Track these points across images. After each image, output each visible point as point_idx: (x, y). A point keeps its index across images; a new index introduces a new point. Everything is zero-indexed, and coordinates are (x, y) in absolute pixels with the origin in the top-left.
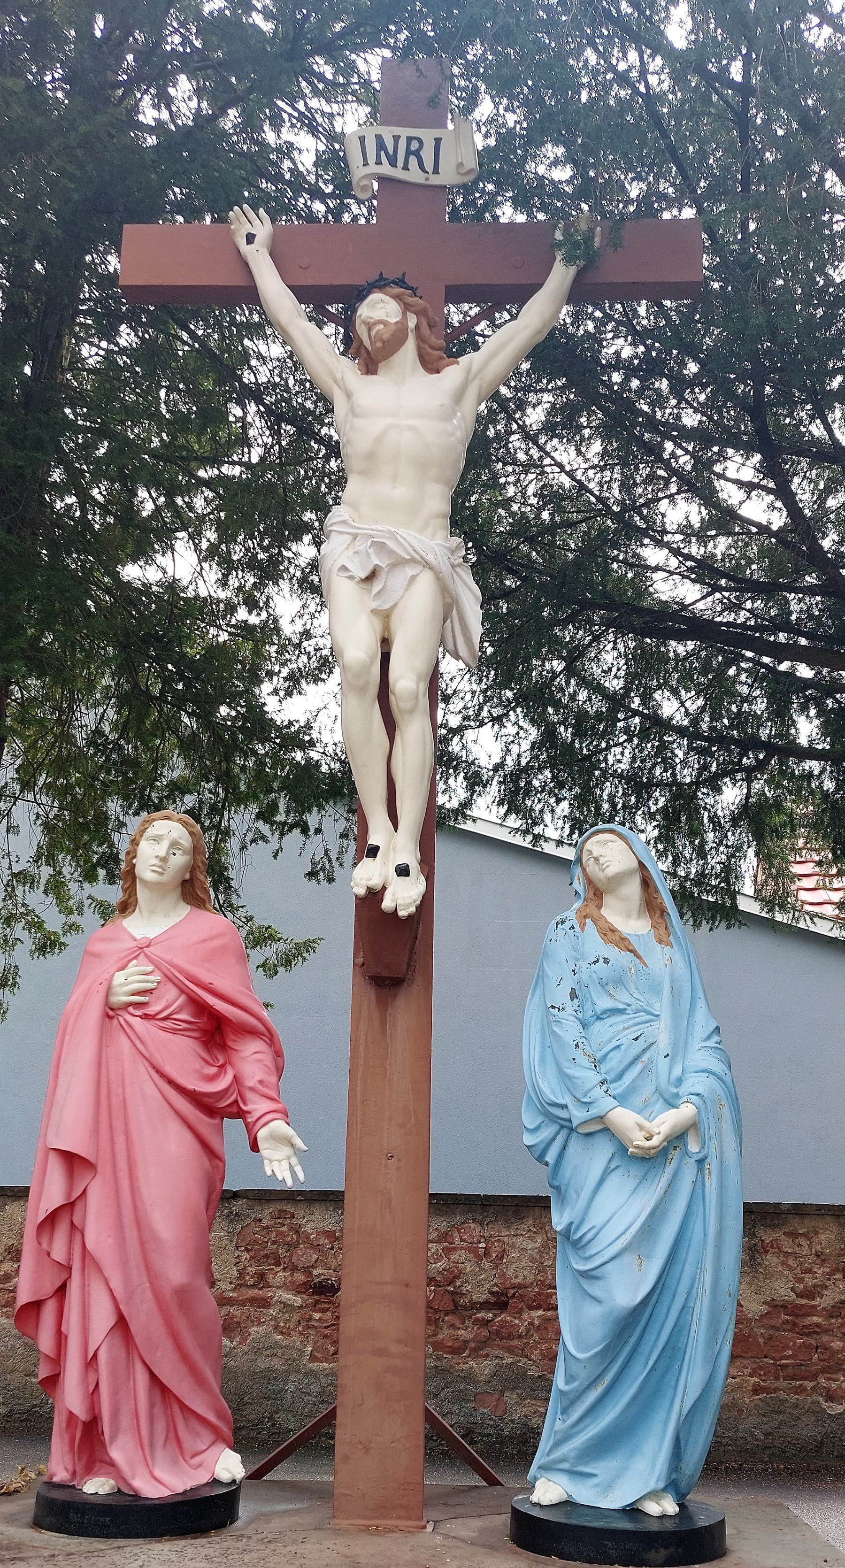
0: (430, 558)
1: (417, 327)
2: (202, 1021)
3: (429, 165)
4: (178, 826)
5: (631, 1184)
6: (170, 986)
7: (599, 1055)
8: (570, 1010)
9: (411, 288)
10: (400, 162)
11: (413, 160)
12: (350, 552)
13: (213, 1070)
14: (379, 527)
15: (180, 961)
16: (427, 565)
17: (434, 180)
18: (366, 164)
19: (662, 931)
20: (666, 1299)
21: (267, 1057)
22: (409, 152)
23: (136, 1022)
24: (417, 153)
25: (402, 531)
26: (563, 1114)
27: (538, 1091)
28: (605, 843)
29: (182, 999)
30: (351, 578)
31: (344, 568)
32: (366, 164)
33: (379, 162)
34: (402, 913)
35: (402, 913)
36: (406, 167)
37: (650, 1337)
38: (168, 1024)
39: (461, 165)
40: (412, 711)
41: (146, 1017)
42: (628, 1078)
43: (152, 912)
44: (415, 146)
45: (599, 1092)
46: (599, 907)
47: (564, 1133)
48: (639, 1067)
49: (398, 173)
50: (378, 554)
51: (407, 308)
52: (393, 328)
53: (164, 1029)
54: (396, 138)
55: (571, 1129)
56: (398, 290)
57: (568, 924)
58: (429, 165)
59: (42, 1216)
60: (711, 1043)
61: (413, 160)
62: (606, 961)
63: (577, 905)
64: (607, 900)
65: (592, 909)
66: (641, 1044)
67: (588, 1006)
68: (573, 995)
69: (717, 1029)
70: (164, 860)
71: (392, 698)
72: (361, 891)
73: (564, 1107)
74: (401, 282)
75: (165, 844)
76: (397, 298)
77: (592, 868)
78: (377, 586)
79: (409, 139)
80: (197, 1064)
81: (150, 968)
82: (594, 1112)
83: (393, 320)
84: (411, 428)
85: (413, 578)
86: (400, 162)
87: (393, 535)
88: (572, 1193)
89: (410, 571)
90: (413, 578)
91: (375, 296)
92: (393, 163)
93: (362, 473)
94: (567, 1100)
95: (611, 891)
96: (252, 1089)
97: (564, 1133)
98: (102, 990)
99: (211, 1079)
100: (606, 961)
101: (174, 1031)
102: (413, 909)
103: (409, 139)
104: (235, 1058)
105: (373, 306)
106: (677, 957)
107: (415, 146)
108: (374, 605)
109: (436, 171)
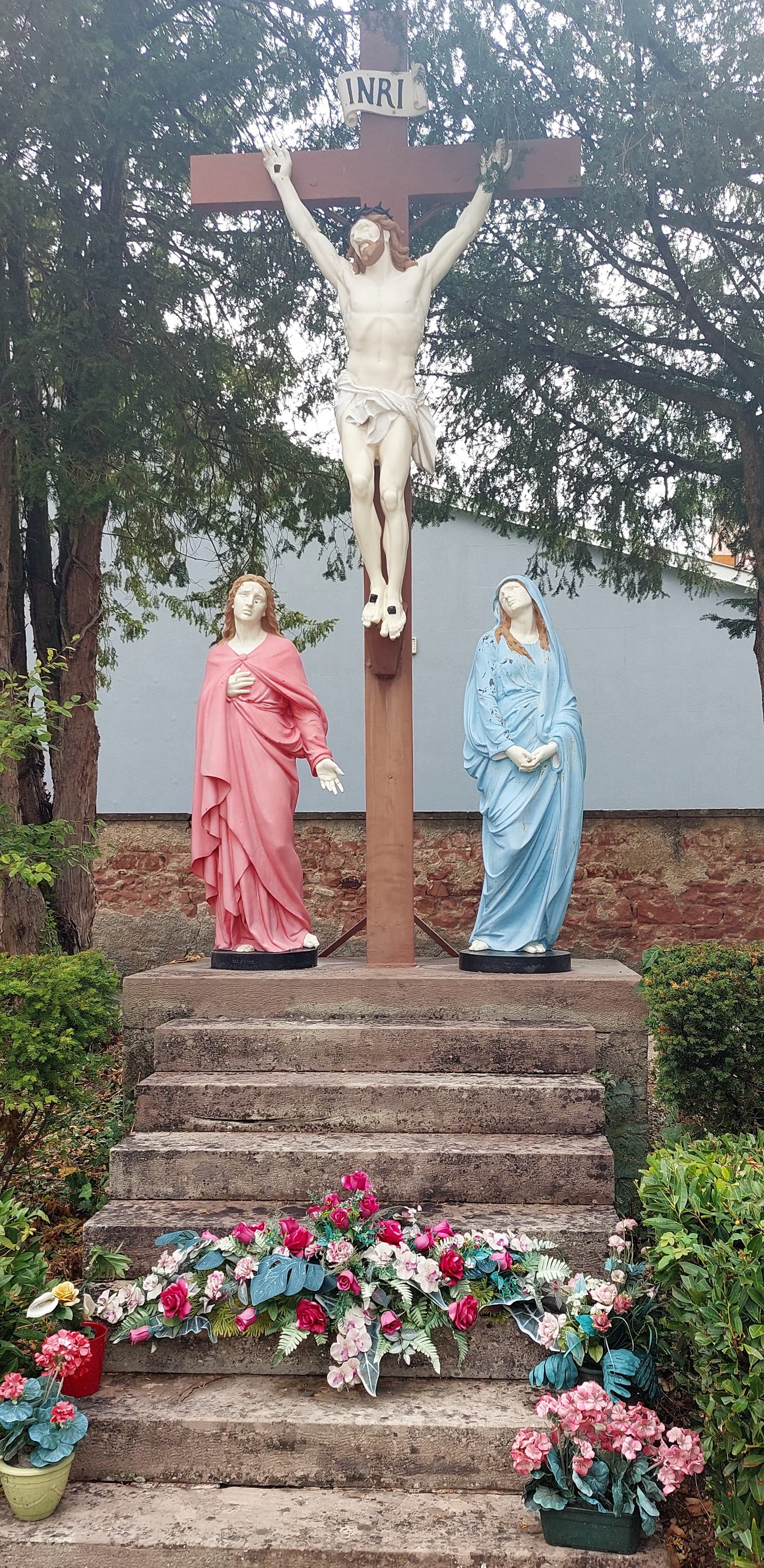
0: (403, 409)
1: (390, 239)
2: (280, 703)
3: (395, 102)
4: (258, 584)
5: (521, 786)
6: (261, 683)
7: (505, 717)
8: (489, 692)
9: (386, 213)
10: (375, 100)
11: (384, 97)
12: (353, 406)
13: (288, 731)
14: (370, 388)
15: (265, 668)
16: (400, 413)
17: (399, 113)
18: (352, 102)
19: (544, 641)
20: (539, 846)
21: (318, 723)
22: (381, 91)
23: (244, 704)
24: (386, 92)
25: (384, 391)
26: (484, 750)
27: (471, 737)
28: (512, 588)
29: (268, 690)
30: (355, 423)
31: (350, 417)
32: (352, 102)
33: (360, 101)
34: (392, 637)
35: (392, 637)
36: (379, 104)
37: (531, 865)
38: (262, 705)
39: (416, 103)
40: (394, 510)
41: (249, 701)
42: (521, 729)
43: (245, 638)
44: (385, 86)
45: (504, 737)
46: (509, 628)
47: (486, 760)
48: (527, 722)
49: (374, 108)
50: (370, 408)
51: (383, 227)
52: (375, 246)
53: (260, 708)
54: (372, 80)
55: (489, 759)
56: (377, 216)
57: (490, 640)
58: (395, 102)
59: (204, 812)
60: (569, 707)
61: (384, 97)
62: (511, 661)
63: (496, 627)
64: (513, 623)
65: (504, 630)
66: (529, 710)
67: (500, 688)
68: (491, 683)
69: (574, 698)
70: (251, 607)
71: (382, 501)
72: (368, 624)
73: (485, 746)
74: (379, 210)
75: (251, 597)
76: (376, 221)
77: (505, 605)
78: (370, 429)
79: (381, 80)
80: (280, 728)
81: (249, 673)
82: (501, 749)
83: (374, 240)
84: (388, 320)
85: (393, 422)
86: (375, 100)
87: (379, 394)
88: (489, 792)
89: (391, 417)
90: (393, 422)
91: (362, 221)
92: (371, 102)
93: (358, 350)
94: (487, 743)
95: (515, 618)
96: (311, 741)
97: (486, 760)
98: (224, 685)
99: (288, 736)
100: (511, 661)
101: (266, 709)
102: (398, 634)
103: (381, 80)
104: (300, 723)
105: (361, 228)
106: (553, 657)
107: (385, 86)
108: (369, 441)
109: (400, 106)
